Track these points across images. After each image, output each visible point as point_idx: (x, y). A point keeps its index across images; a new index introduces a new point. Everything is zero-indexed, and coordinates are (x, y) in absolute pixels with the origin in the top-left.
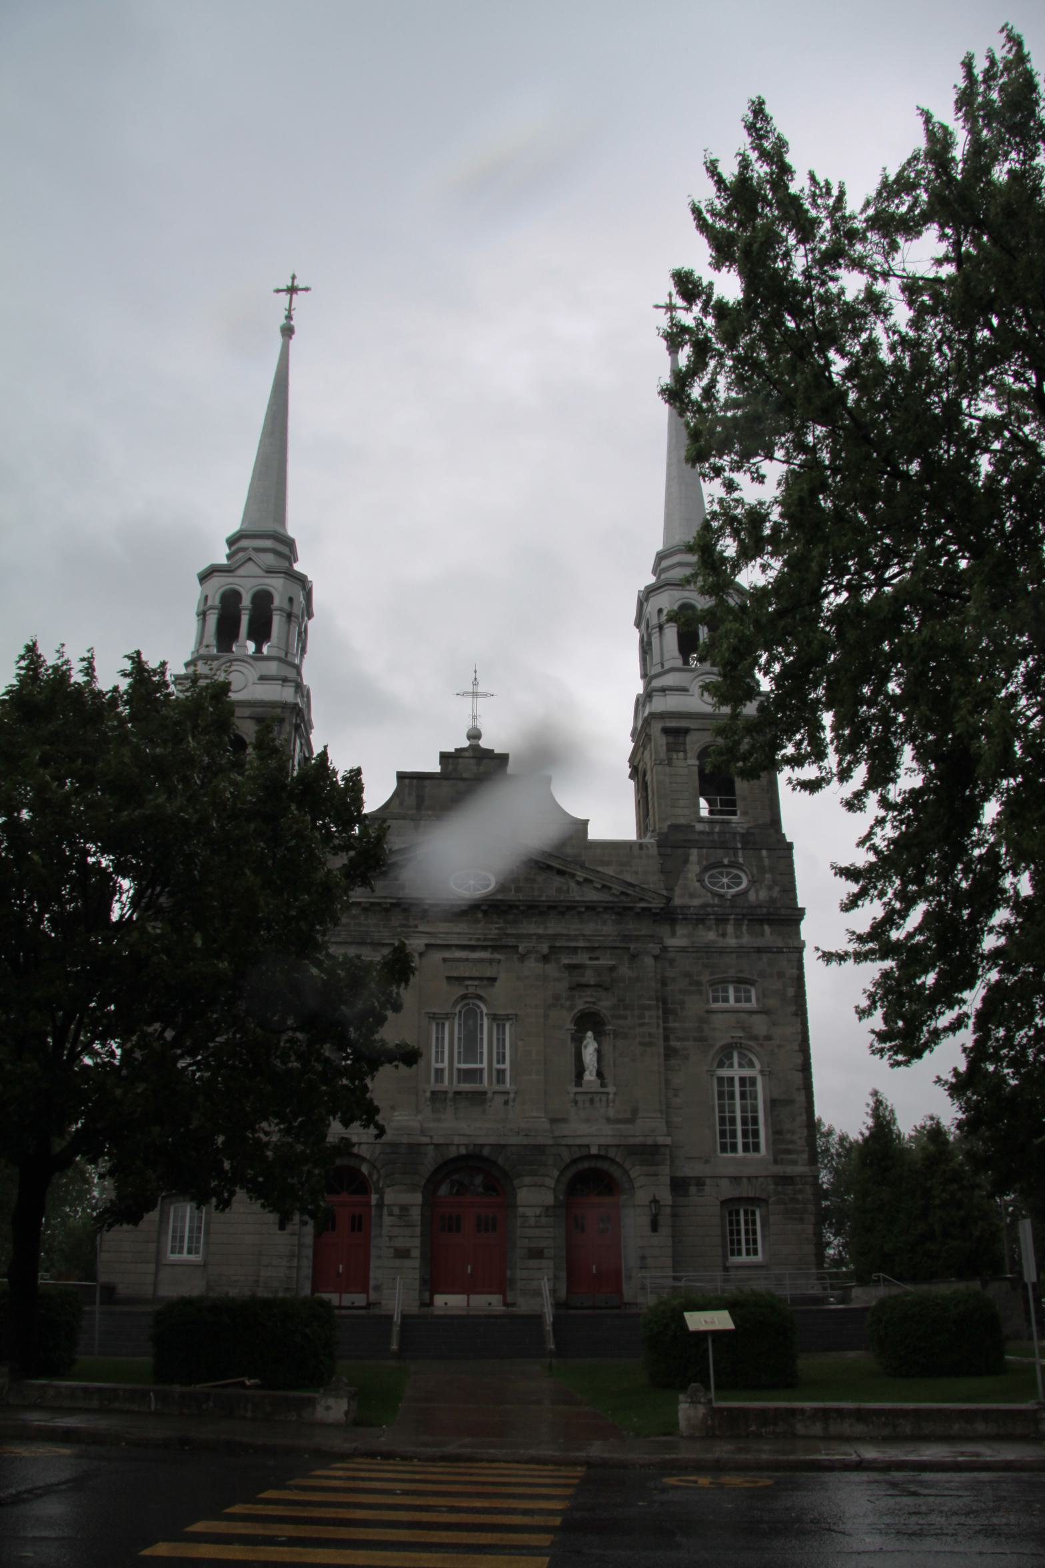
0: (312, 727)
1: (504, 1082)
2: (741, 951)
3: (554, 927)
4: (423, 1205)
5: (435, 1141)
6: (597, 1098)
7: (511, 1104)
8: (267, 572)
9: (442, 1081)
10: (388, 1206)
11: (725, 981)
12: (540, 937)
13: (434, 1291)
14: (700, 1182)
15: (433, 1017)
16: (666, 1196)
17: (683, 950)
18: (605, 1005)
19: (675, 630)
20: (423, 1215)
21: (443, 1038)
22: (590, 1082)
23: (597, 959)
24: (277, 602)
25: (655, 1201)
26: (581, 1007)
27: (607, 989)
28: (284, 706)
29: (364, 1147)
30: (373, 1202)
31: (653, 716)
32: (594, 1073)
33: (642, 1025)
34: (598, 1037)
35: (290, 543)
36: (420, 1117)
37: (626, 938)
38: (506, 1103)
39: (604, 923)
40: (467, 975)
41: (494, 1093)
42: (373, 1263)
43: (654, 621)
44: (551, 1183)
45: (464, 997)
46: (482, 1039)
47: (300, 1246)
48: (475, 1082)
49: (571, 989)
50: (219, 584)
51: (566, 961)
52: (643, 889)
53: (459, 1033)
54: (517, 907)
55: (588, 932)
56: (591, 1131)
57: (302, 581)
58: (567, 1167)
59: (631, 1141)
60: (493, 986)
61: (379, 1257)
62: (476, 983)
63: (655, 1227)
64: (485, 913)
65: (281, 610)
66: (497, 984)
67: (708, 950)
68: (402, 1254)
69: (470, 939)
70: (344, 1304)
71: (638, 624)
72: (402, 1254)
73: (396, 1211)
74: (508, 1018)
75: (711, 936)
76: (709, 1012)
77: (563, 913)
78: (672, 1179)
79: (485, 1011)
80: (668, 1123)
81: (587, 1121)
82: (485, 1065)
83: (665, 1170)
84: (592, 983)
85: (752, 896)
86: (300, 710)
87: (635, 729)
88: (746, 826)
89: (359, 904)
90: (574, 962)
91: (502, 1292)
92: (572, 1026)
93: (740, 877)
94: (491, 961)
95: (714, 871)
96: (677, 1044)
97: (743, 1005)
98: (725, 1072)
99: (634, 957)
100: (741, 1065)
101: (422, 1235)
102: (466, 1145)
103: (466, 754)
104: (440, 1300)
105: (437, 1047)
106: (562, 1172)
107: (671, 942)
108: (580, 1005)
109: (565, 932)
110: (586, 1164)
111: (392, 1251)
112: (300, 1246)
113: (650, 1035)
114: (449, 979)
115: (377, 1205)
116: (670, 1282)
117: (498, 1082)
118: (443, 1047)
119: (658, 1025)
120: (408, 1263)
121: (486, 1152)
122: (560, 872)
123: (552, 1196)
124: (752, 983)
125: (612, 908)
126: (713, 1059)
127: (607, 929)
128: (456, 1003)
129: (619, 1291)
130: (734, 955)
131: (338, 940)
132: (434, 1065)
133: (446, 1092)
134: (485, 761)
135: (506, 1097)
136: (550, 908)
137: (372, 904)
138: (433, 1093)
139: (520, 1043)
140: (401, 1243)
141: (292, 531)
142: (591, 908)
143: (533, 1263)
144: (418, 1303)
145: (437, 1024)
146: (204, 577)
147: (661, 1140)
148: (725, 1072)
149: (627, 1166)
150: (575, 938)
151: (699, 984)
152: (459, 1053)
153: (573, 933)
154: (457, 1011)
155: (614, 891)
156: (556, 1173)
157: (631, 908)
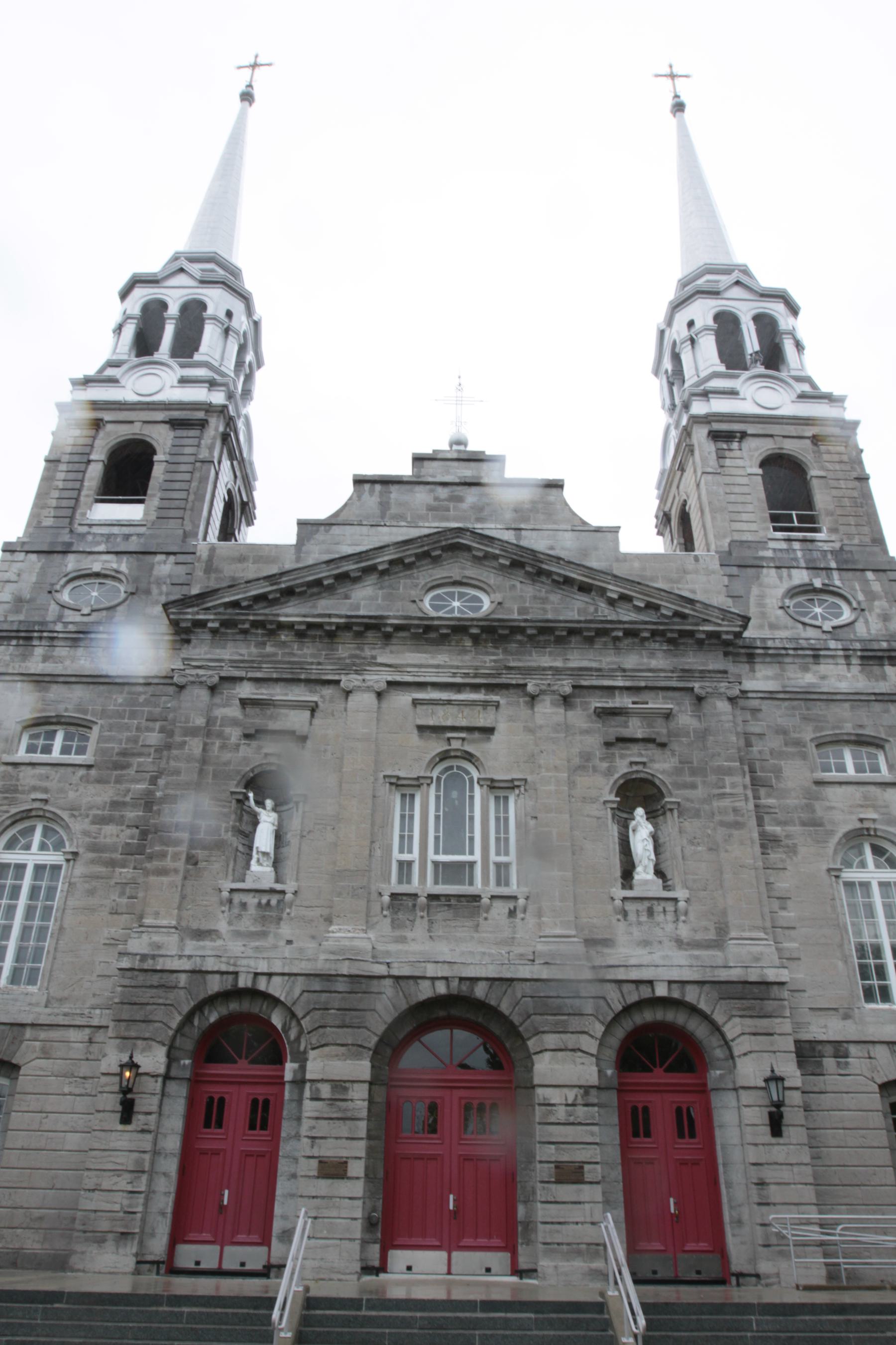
0: (255, 479)
1: (507, 884)
2: (857, 699)
3: (578, 658)
4: (371, 1083)
5: (395, 972)
6: (658, 908)
7: (520, 915)
8: (202, 282)
9: (409, 882)
10: (310, 1081)
11: (838, 741)
12: (557, 671)
13: (387, 1245)
14: (840, 1049)
15: (396, 783)
16: (789, 1069)
17: (770, 696)
18: (661, 767)
19: (713, 337)
20: (371, 1101)
21: (411, 817)
22: (646, 882)
23: (647, 703)
24: (210, 311)
25: (775, 1079)
26: (626, 770)
27: (663, 745)
28: (209, 408)
29: (276, 980)
30: (288, 1076)
31: (696, 420)
32: (652, 871)
33: (723, 796)
34: (651, 816)
35: (235, 272)
36: (371, 935)
37: (687, 673)
38: (512, 913)
39: (652, 655)
40: (449, 723)
41: (493, 897)
42: (282, 1186)
43: (685, 333)
44: (591, 1045)
45: (444, 756)
46: (472, 818)
47: (156, 1152)
48: (461, 882)
49: (608, 744)
50: (140, 295)
51: (597, 702)
52: (707, 606)
53: (437, 809)
54: (521, 630)
55: (627, 666)
56: (658, 958)
57: (245, 298)
58: (617, 1018)
59: (723, 975)
60: (489, 739)
61: (294, 1176)
62: (463, 735)
63: (776, 1125)
64: (476, 639)
65: (214, 318)
66: (495, 738)
67: (807, 697)
68: (332, 1170)
69: (454, 675)
70: (227, 1266)
71: (656, 372)
72: (332, 1170)
73: (325, 1091)
74: (512, 786)
75: (808, 679)
76: (819, 783)
77: (590, 641)
78: (795, 1042)
79: (475, 775)
80: (777, 949)
81: (646, 943)
82: (477, 856)
83: (786, 1026)
84: (639, 735)
85: (861, 629)
86: (231, 419)
87: (662, 473)
88: (837, 545)
89: (290, 626)
90: (610, 705)
91: (511, 1248)
92: (612, 797)
93: (839, 607)
94: (485, 704)
95: (801, 599)
96: (778, 829)
97: (868, 776)
98: (852, 875)
99: (700, 699)
100: (877, 866)
101: (369, 1137)
102: (446, 979)
103: (449, 456)
104: (399, 1258)
105: (402, 829)
106: (609, 1027)
107: (749, 685)
108: (622, 767)
109: (594, 665)
110: (648, 1016)
111: (314, 1163)
112: (156, 1152)
113: (735, 810)
114: (421, 729)
115: (292, 1082)
116: (814, 1234)
117: (498, 884)
118: (411, 830)
119: (747, 799)
120: (343, 1188)
121: (480, 991)
122: (585, 588)
123: (595, 1069)
124: (877, 743)
125: (662, 633)
126: (836, 852)
127: (656, 661)
128: (432, 764)
129: (720, 1249)
130: (847, 705)
131: (259, 675)
132: (396, 855)
133: (415, 896)
134: (472, 464)
135: (511, 905)
136: (572, 632)
137: (310, 626)
138: (394, 896)
139: (532, 823)
140: (330, 1150)
141: (240, 258)
142: (631, 633)
143: (566, 1191)
144: (357, 1267)
145: (403, 796)
146: (124, 295)
147: (772, 975)
148: (852, 875)
149: (719, 1018)
150: (610, 673)
151: (798, 743)
152: (437, 838)
153: (604, 666)
154: (435, 774)
155: (664, 611)
156: (599, 1029)
157: (691, 634)
